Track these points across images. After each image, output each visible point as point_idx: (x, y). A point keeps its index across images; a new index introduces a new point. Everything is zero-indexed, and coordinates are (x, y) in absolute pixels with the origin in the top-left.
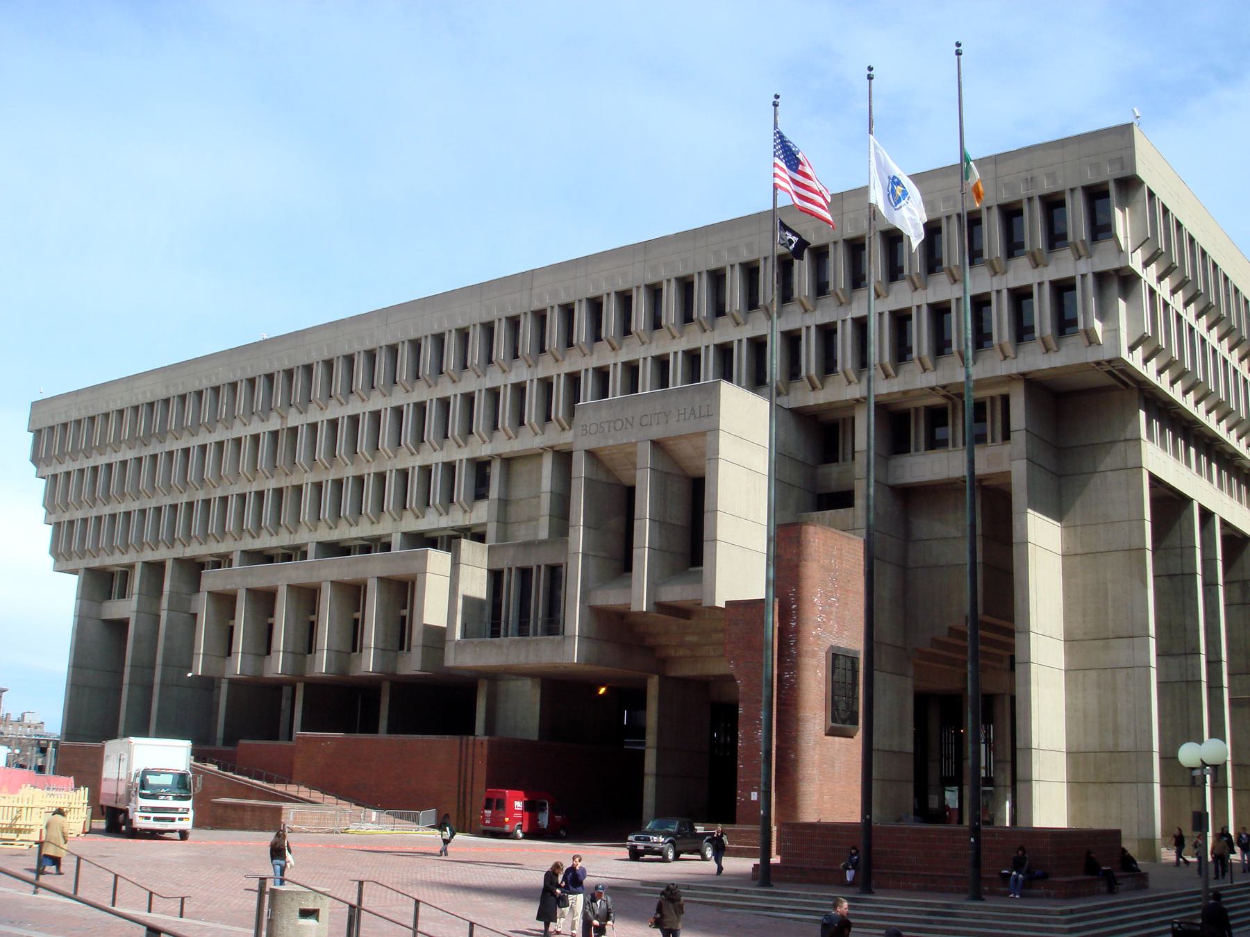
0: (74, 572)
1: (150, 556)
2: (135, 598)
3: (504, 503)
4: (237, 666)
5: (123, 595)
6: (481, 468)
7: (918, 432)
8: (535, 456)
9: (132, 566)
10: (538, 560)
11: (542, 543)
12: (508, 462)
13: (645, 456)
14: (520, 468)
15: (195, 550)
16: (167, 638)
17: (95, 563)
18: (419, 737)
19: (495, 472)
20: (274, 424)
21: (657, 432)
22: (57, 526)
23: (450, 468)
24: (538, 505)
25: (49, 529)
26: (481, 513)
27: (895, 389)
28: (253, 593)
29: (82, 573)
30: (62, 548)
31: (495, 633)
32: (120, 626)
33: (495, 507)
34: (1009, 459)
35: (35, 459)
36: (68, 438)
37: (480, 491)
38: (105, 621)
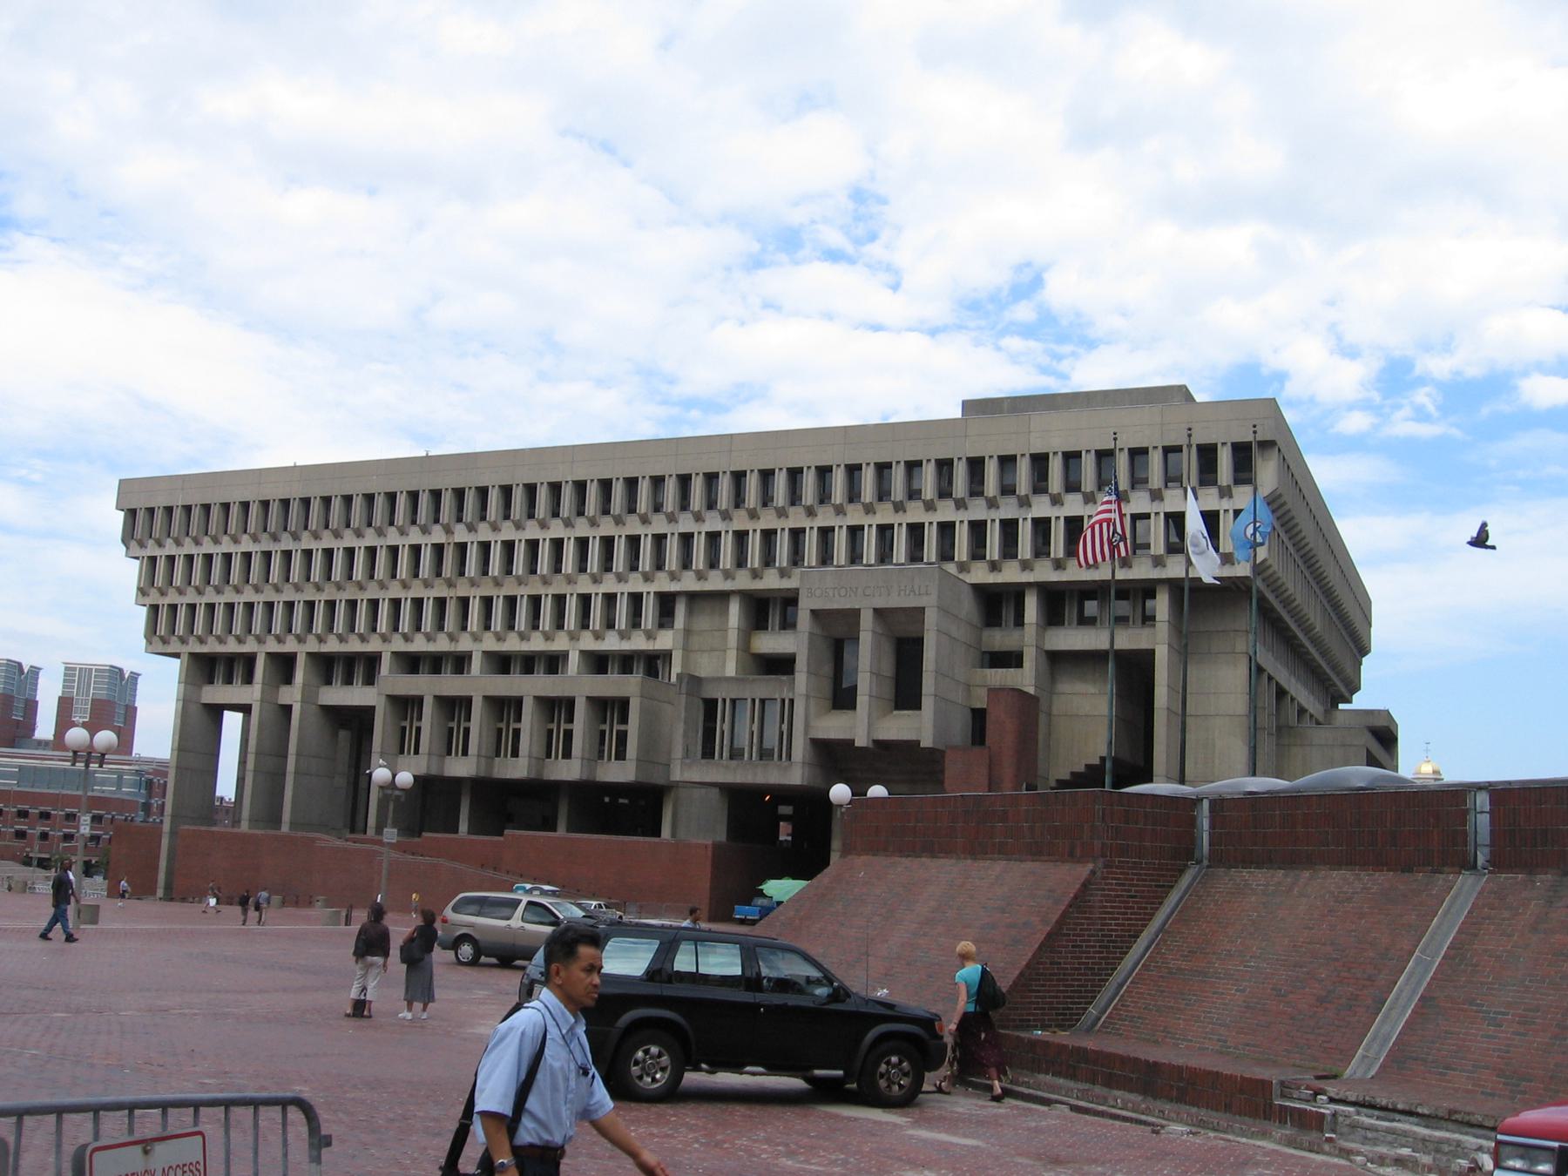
0: (177, 655)
3: (687, 632)
6: (666, 603)
7: (1070, 612)
8: (723, 597)
9: (250, 660)
12: (693, 597)
22: (154, 609)
24: (725, 638)
25: (143, 612)
26: (665, 640)
27: (1064, 579)
29: (185, 657)
30: (162, 629)
33: (681, 636)
34: (1158, 639)
38: (206, 705)
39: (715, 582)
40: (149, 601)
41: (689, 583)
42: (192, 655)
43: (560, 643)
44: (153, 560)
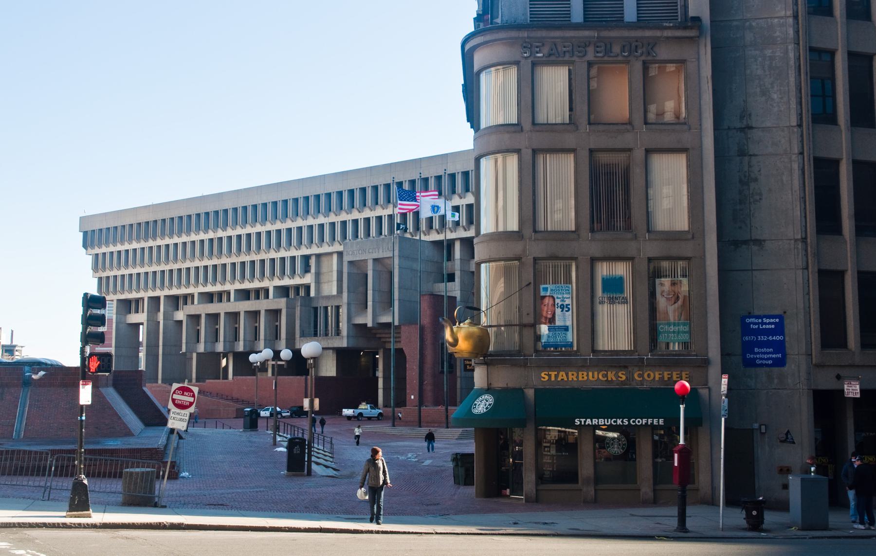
1: (151, 294)
2: (145, 314)
3: (318, 275)
4: (201, 348)
5: (137, 312)
6: (306, 258)
8: (330, 254)
9: (143, 299)
10: (331, 304)
11: (333, 296)
12: (319, 256)
13: (370, 265)
14: (325, 260)
15: (175, 292)
16: (164, 333)
17: (123, 297)
18: (287, 377)
19: (313, 262)
20: (211, 235)
21: (376, 256)
22: (100, 279)
23: (293, 258)
26: (309, 279)
28: (208, 315)
31: (316, 335)
32: (137, 326)
35: (85, 246)
36: (82, 219)
37: (307, 269)
39: (325, 249)
40: (98, 275)
41: (315, 250)
42: (118, 300)
43: (266, 283)
44: (97, 255)
